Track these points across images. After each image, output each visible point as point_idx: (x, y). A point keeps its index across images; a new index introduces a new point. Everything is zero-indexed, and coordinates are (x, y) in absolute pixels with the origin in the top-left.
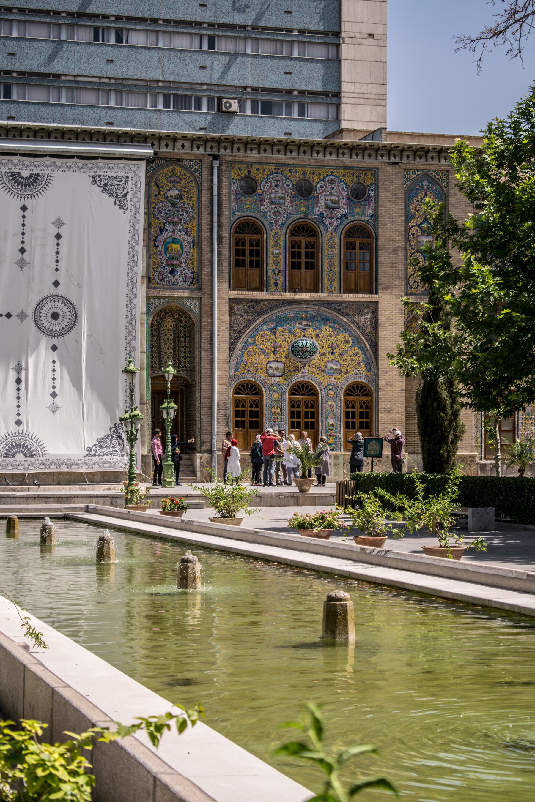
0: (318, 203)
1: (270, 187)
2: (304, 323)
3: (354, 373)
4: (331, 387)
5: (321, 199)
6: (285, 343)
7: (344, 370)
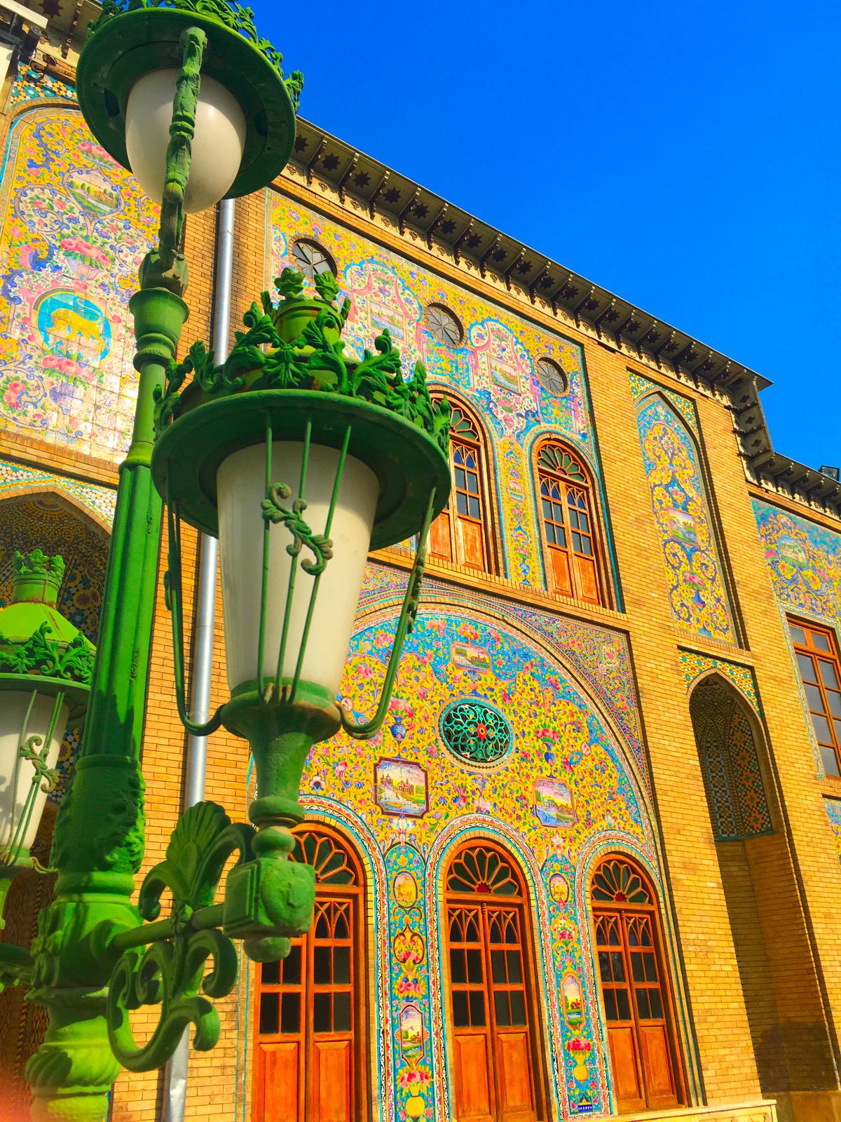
0: (476, 366)
1: (369, 287)
2: (472, 652)
3: (604, 824)
4: (557, 867)
5: (483, 359)
6: (426, 704)
7: (581, 812)
